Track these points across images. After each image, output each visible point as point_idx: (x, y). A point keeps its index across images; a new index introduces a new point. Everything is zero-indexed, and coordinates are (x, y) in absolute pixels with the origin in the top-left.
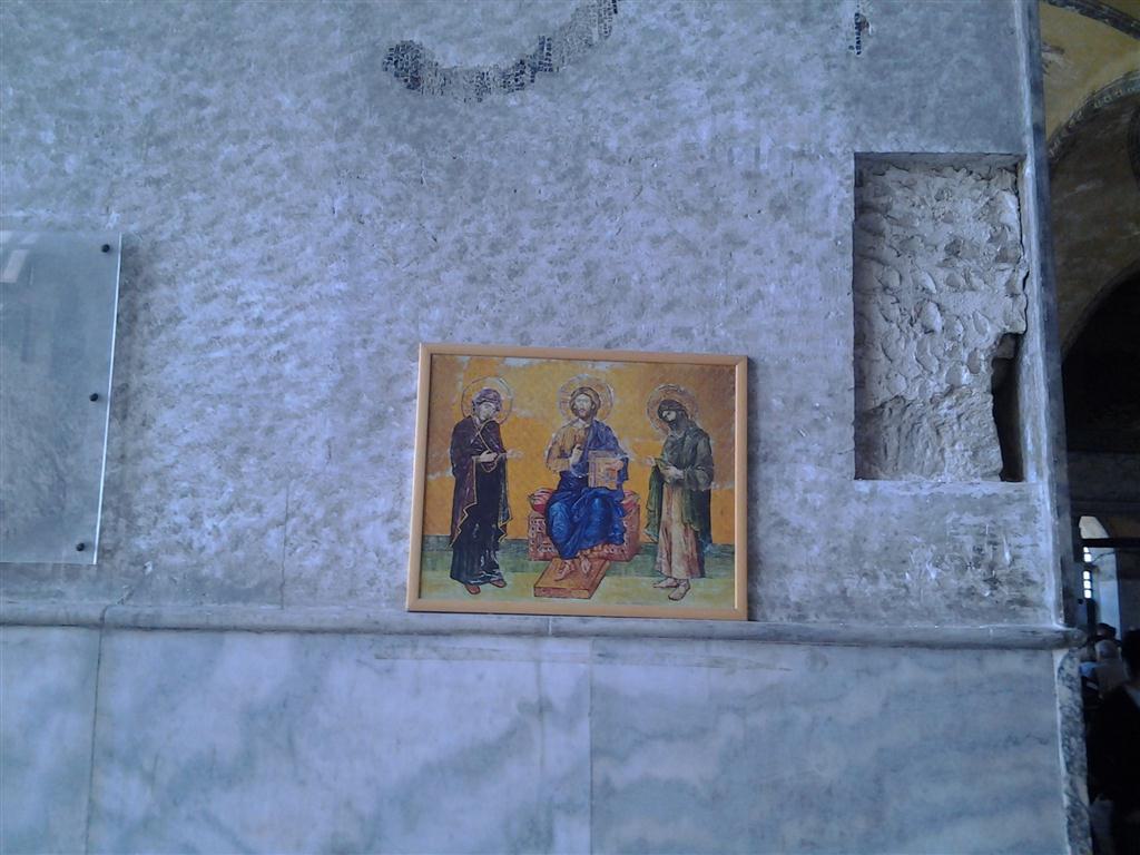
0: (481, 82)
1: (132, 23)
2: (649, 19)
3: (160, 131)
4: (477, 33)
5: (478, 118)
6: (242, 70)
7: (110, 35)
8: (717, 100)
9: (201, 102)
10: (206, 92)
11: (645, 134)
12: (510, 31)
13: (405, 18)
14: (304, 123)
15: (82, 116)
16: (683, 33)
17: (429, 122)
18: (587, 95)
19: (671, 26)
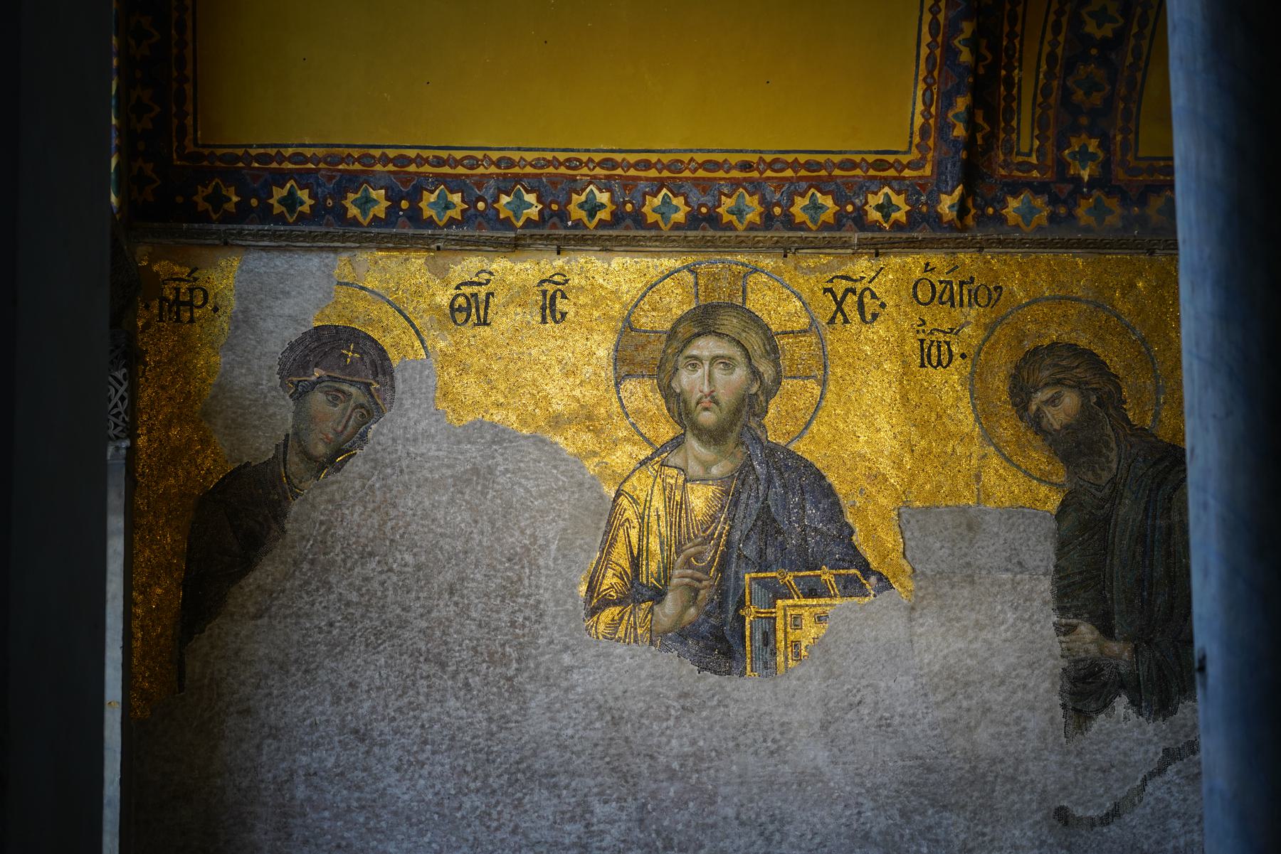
0: (1092, 823)
1: (953, 801)
2: (1158, 794)
3: (970, 845)
4: (1090, 801)
5: (1092, 838)
6: (998, 821)
7: (945, 807)
8: (1186, 828)
9: (984, 835)
10: (985, 830)
11: (1158, 843)
12: (1102, 800)
13: (1061, 796)
14: (1024, 843)
15: (937, 841)
16: (1172, 800)
17: (1073, 840)
18: (1135, 827)
19: (1167, 796)
